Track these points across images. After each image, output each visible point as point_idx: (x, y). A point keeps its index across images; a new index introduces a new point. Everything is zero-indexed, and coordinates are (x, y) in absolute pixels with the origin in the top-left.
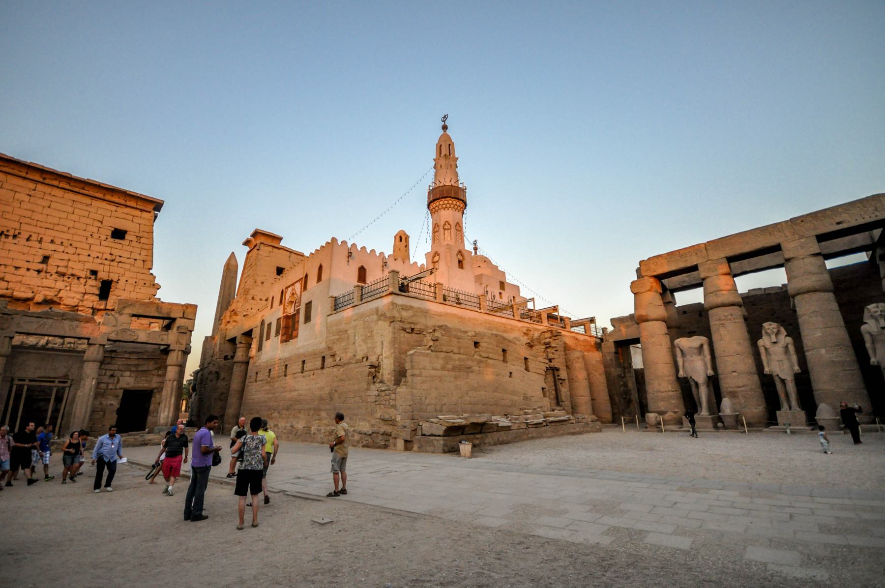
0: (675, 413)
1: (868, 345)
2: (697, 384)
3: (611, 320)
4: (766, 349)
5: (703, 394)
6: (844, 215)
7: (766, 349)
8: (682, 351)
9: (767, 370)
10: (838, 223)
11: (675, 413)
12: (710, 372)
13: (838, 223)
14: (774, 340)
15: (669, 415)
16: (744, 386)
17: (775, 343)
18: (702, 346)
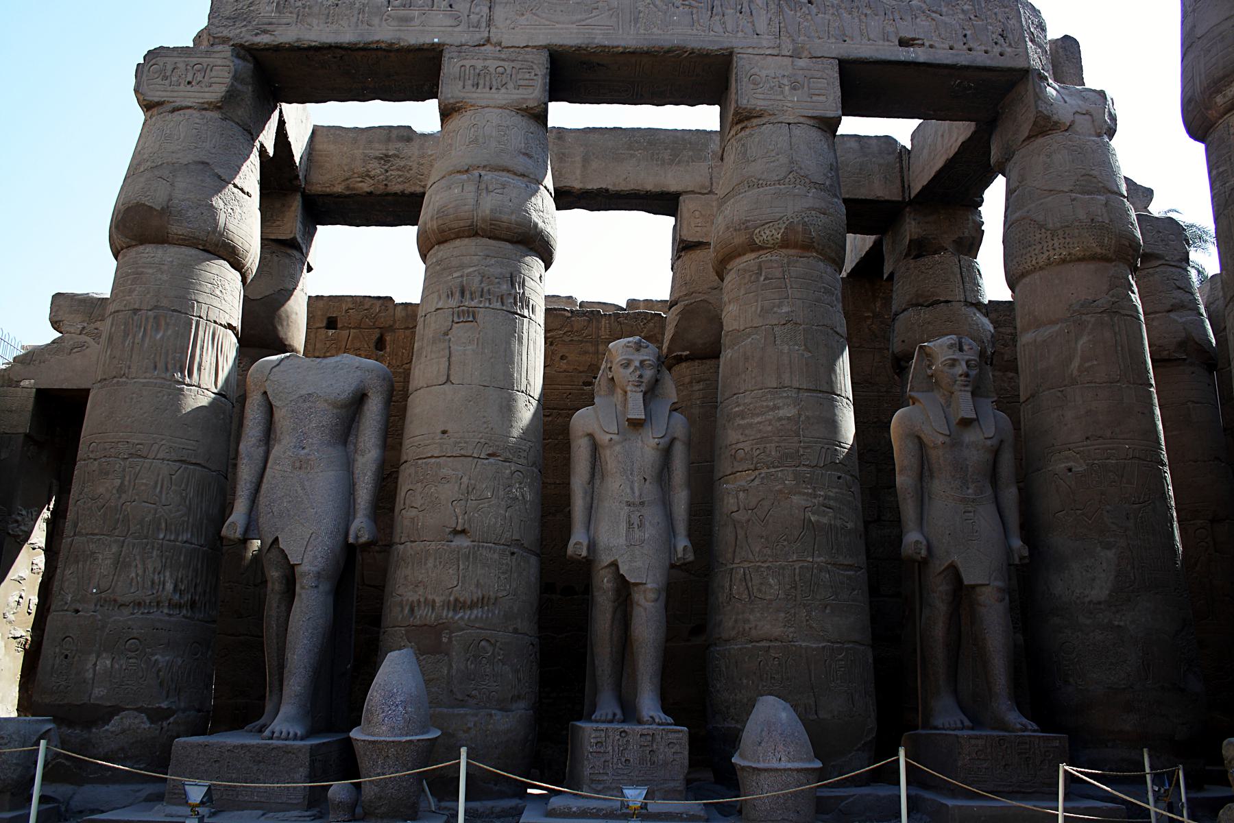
0: (156, 716)
1: (903, 480)
2: (290, 576)
3: (58, 298)
4: (595, 448)
5: (305, 624)
6: (922, 22)
7: (595, 448)
8: (270, 409)
9: (578, 541)
10: (903, 43)
11: (156, 716)
12: (361, 528)
13: (903, 43)
14: (637, 412)
15: (131, 724)
16: (482, 602)
17: (636, 424)
18: (359, 399)
